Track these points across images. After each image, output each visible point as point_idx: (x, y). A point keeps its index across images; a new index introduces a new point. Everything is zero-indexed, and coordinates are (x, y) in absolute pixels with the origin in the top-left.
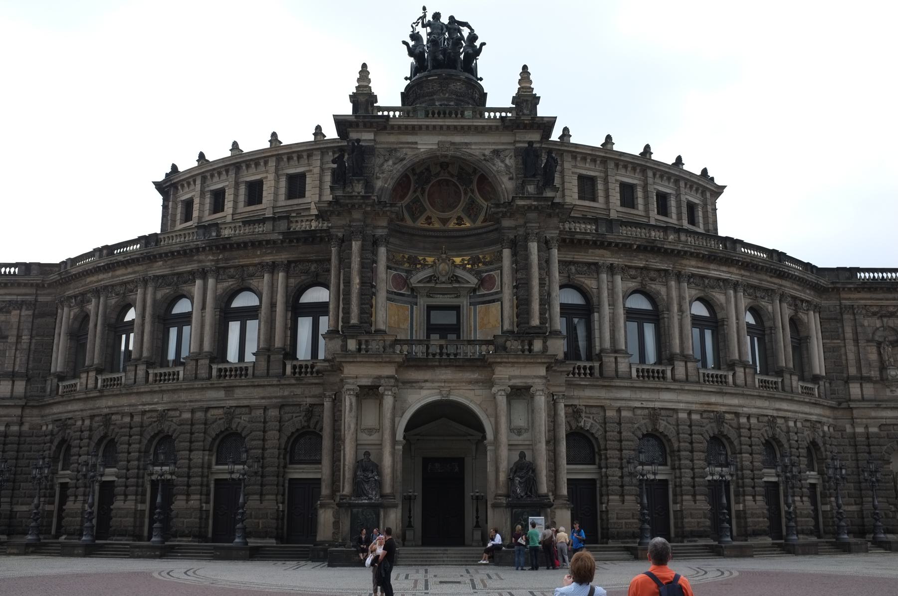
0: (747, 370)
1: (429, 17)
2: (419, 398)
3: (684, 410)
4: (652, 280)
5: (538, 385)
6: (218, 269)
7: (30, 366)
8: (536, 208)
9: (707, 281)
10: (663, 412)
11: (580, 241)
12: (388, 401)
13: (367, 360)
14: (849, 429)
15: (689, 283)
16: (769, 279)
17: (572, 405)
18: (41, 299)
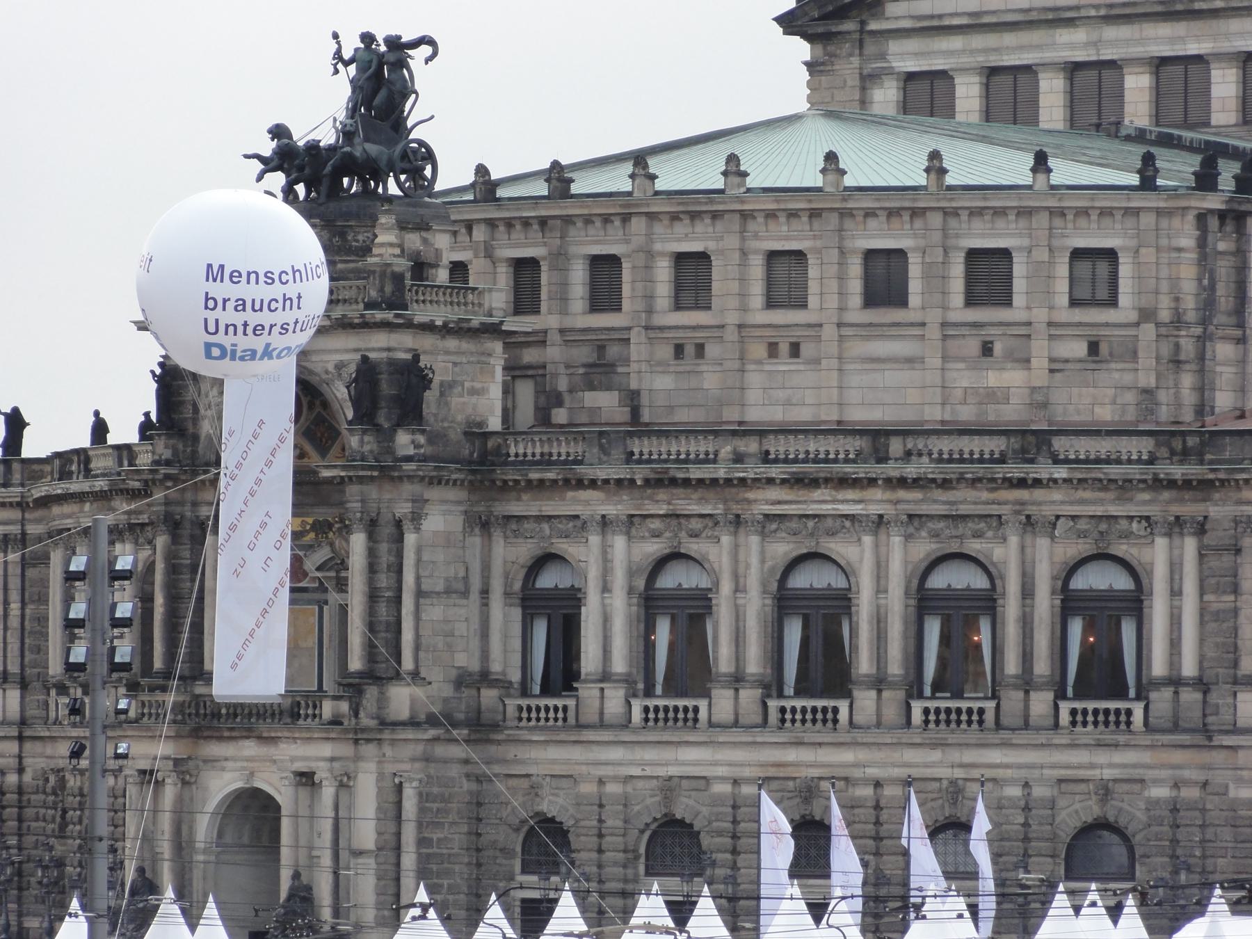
0: (885, 694)
1: (351, 45)
2: (220, 785)
3: (723, 779)
4: (695, 535)
5: (322, 772)
6: (132, 527)
7: (27, 660)
8: (350, 478)
9: (811, 524)
10: (685, 783)
11: (541, 482)
12: (170, 793)
13: (136, 733)
14: (1232, 793)
15: (763, 534)
16: (985, 495)
17: (528, 776)
18: (32, 529)
